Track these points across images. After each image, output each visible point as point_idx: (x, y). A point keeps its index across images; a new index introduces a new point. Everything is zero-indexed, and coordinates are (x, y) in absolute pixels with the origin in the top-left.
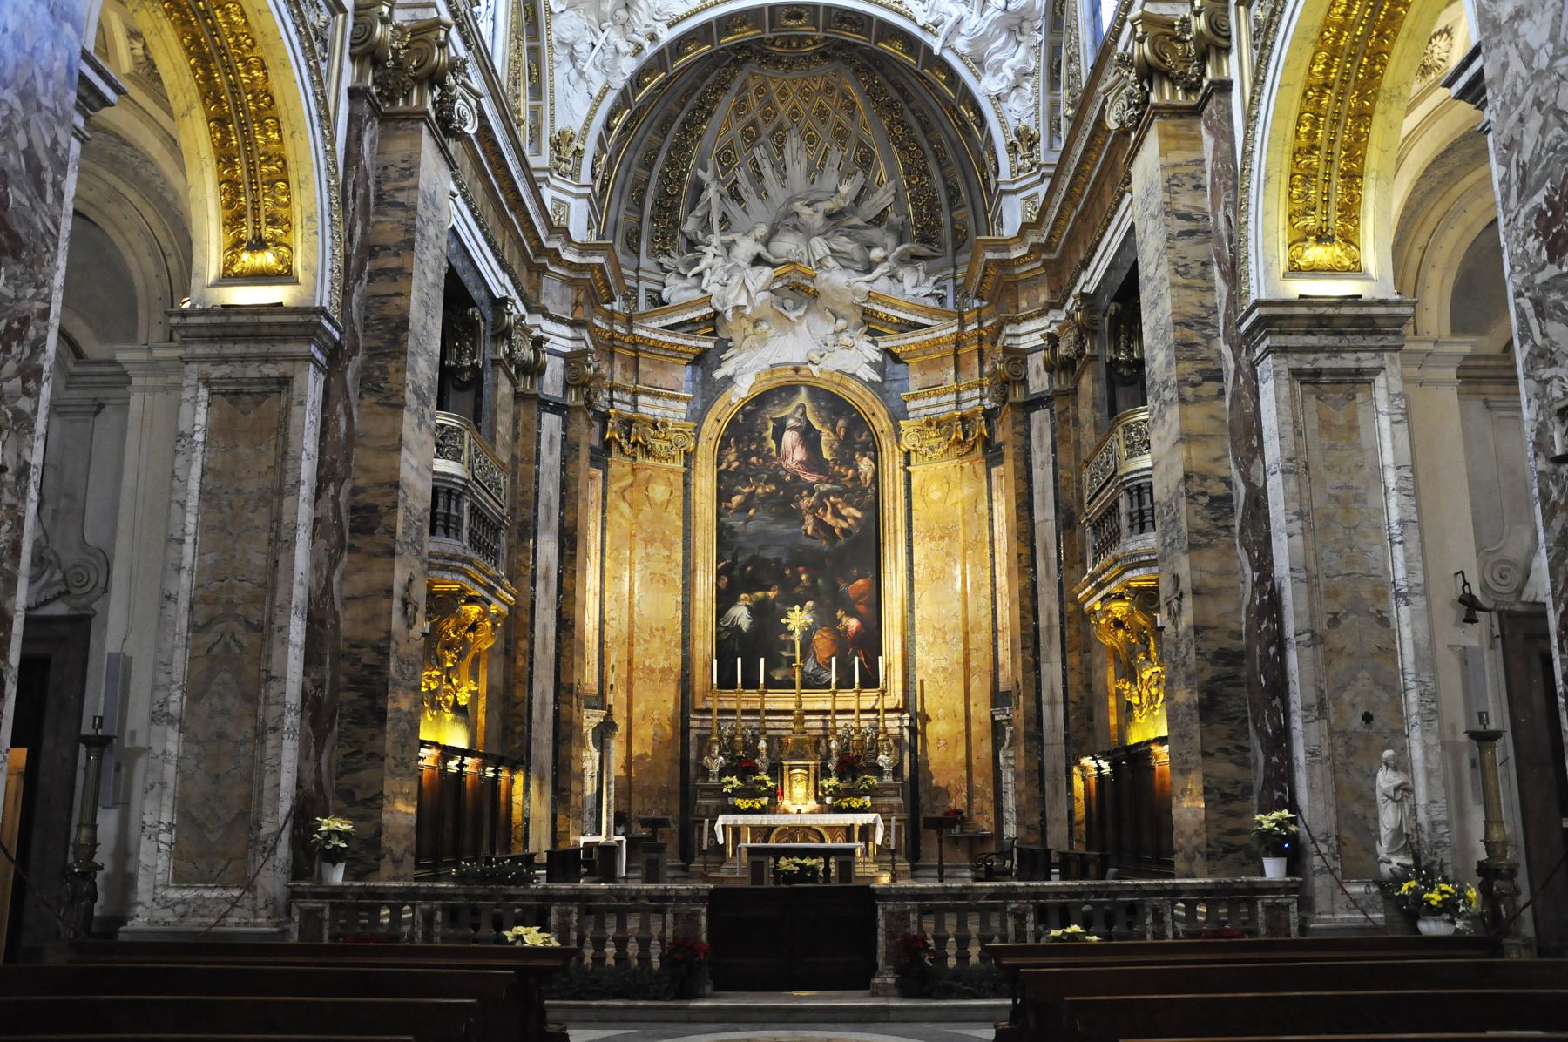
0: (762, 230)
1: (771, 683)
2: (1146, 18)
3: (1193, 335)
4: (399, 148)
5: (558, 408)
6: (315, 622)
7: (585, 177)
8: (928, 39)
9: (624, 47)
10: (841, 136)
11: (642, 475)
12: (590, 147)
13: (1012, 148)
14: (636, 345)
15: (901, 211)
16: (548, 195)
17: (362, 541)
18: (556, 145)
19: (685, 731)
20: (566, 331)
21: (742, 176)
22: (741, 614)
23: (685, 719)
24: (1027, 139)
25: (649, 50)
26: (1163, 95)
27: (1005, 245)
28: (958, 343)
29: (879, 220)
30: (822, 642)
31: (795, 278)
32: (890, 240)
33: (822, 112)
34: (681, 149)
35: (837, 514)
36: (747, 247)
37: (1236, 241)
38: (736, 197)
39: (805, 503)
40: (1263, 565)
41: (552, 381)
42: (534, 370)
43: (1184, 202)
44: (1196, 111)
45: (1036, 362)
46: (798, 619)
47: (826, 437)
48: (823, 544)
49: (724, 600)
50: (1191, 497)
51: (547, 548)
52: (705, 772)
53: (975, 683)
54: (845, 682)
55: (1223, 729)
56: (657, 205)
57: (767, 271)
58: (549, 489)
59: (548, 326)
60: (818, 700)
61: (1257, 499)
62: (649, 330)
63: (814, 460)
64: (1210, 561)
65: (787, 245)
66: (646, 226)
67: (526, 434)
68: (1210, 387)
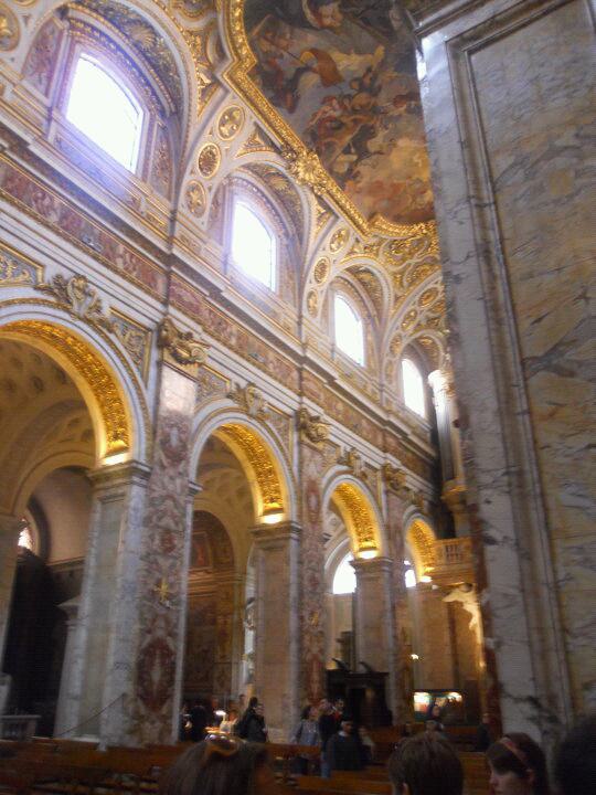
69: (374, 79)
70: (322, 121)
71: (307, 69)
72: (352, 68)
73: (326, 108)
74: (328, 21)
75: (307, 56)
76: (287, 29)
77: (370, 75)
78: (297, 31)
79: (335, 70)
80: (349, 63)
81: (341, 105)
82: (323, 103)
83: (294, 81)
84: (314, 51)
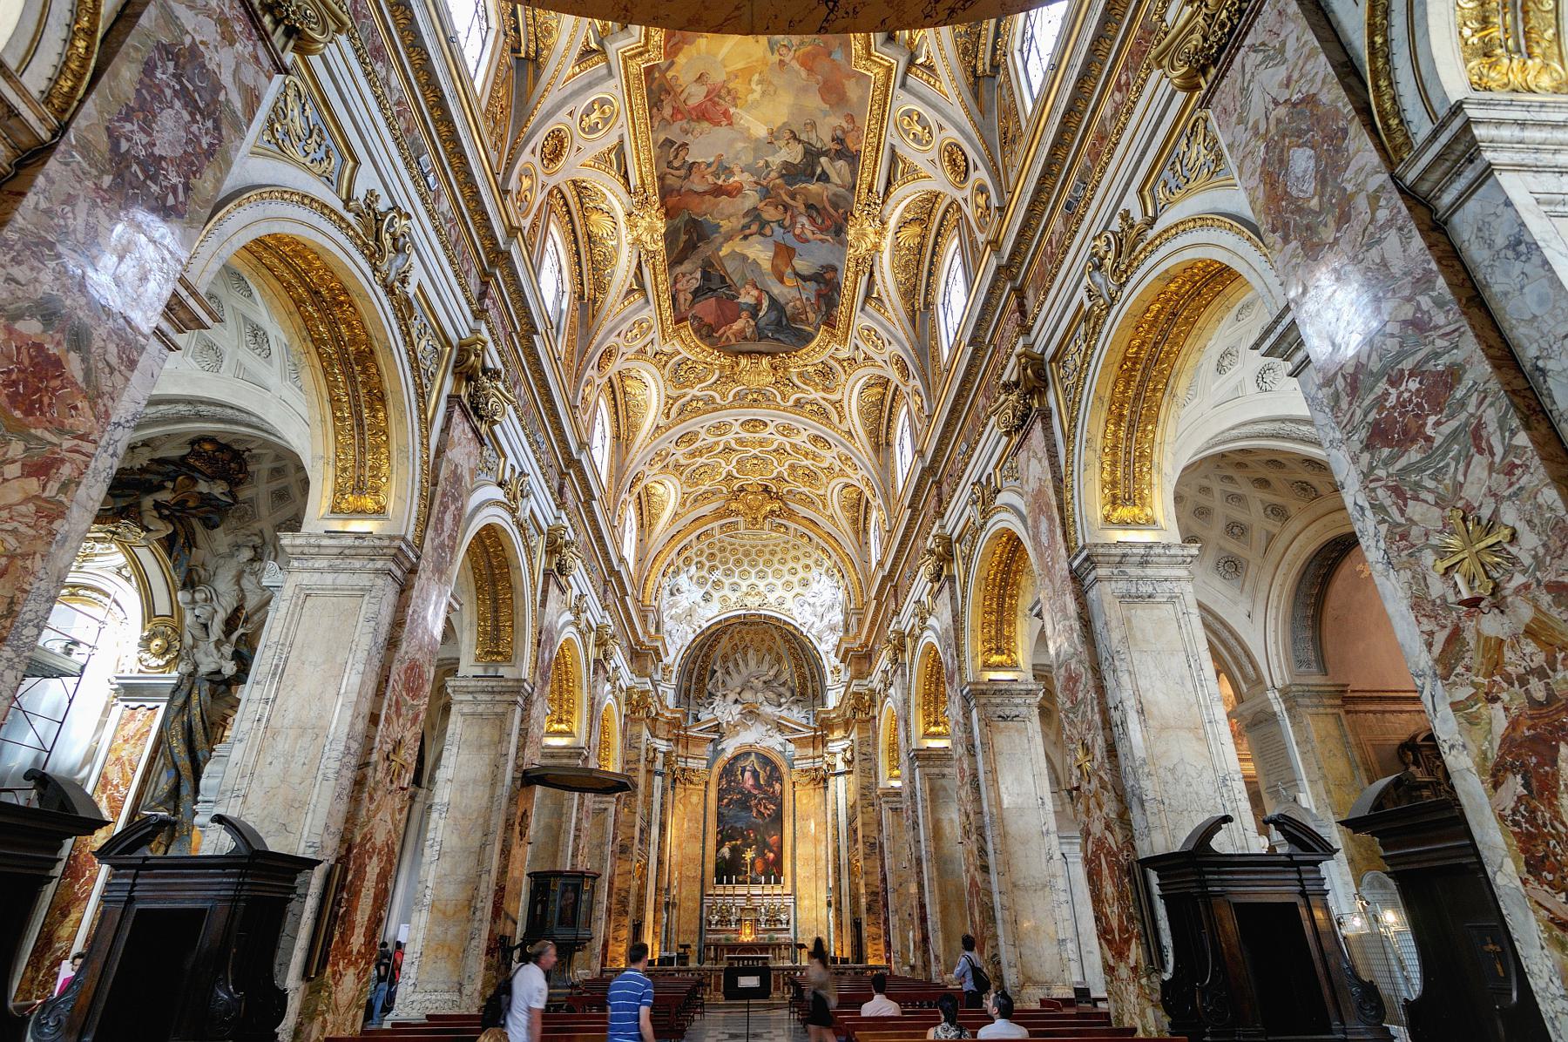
0: (738, 690)
1: (738, 882)
2: (854, 693)
3: (866, 792)
4: (636, 729)
5: (661, 774)
6: (611, 883)
7: (674, 681)
8: (802, 629)
9: (690, 631)
10: (770, 650)
11: (688, 792)
12: (675, 668)
13: (832, 672)
14: (687, 737)
15: (793, 682)
16: (660, 689)
17: (623, 856)
18: (663, 670)
19: (702, 905)
20: (665, 743)
21: (731, 665)
22: (726, 851)
23: (702, 899)
24: (836, 670)
25: (698, 631)
26: (860, 716)
27: (829, 712)
28: (814, 737)
29: (784, 684)
30: (759, 865)
31: (751, 708)
32: (788, 694)
33: (763, 640)
34: (707, 655)
35: (766, 808)
36: (732, 697)
37: (876, 765)
38: (728, 673)
39: (753, 803)
40: (883, 866)
41: (659, 765)
42: (653, 761)
43: (864, 750)
44: (868, 721)
45: (839, 757)
46: (749, 855)
47: (762, 774)
48: (760, 821)
49: (720, 845)
50: (864, 843)
51: (655, 831)
52: (710, 923)
53: (820, 883)
54: (768, 882)
55: (873, 917)
56: (697, 678)
57: (740, 707)
58: (657, 807)
59: (658, 741)
60: (756, 890)
61: (881, 846)
62: (693, 732)
63: (757, 785)
64: (869, 863)
65: (748, 696)
66: (693, 687)
67: (649, 785)
68: (871, 809)
69: (744, 227)
70: (822, 231)
71: (797, 274)
72: (759, 247)
73: (809, 235)
74: (755, 293)
75: (790, 281)
76: (789, 310)
77: (747, 232)
78: (782, 301)
79: (776, 255)
80: (760, 252)
81: (793, 224)
82: (807, 241)
83: (815, 278)
84: (782, 282)
